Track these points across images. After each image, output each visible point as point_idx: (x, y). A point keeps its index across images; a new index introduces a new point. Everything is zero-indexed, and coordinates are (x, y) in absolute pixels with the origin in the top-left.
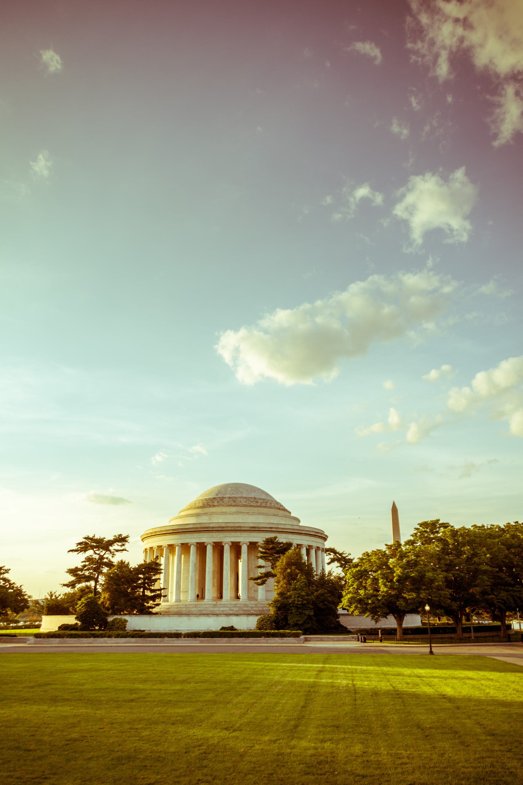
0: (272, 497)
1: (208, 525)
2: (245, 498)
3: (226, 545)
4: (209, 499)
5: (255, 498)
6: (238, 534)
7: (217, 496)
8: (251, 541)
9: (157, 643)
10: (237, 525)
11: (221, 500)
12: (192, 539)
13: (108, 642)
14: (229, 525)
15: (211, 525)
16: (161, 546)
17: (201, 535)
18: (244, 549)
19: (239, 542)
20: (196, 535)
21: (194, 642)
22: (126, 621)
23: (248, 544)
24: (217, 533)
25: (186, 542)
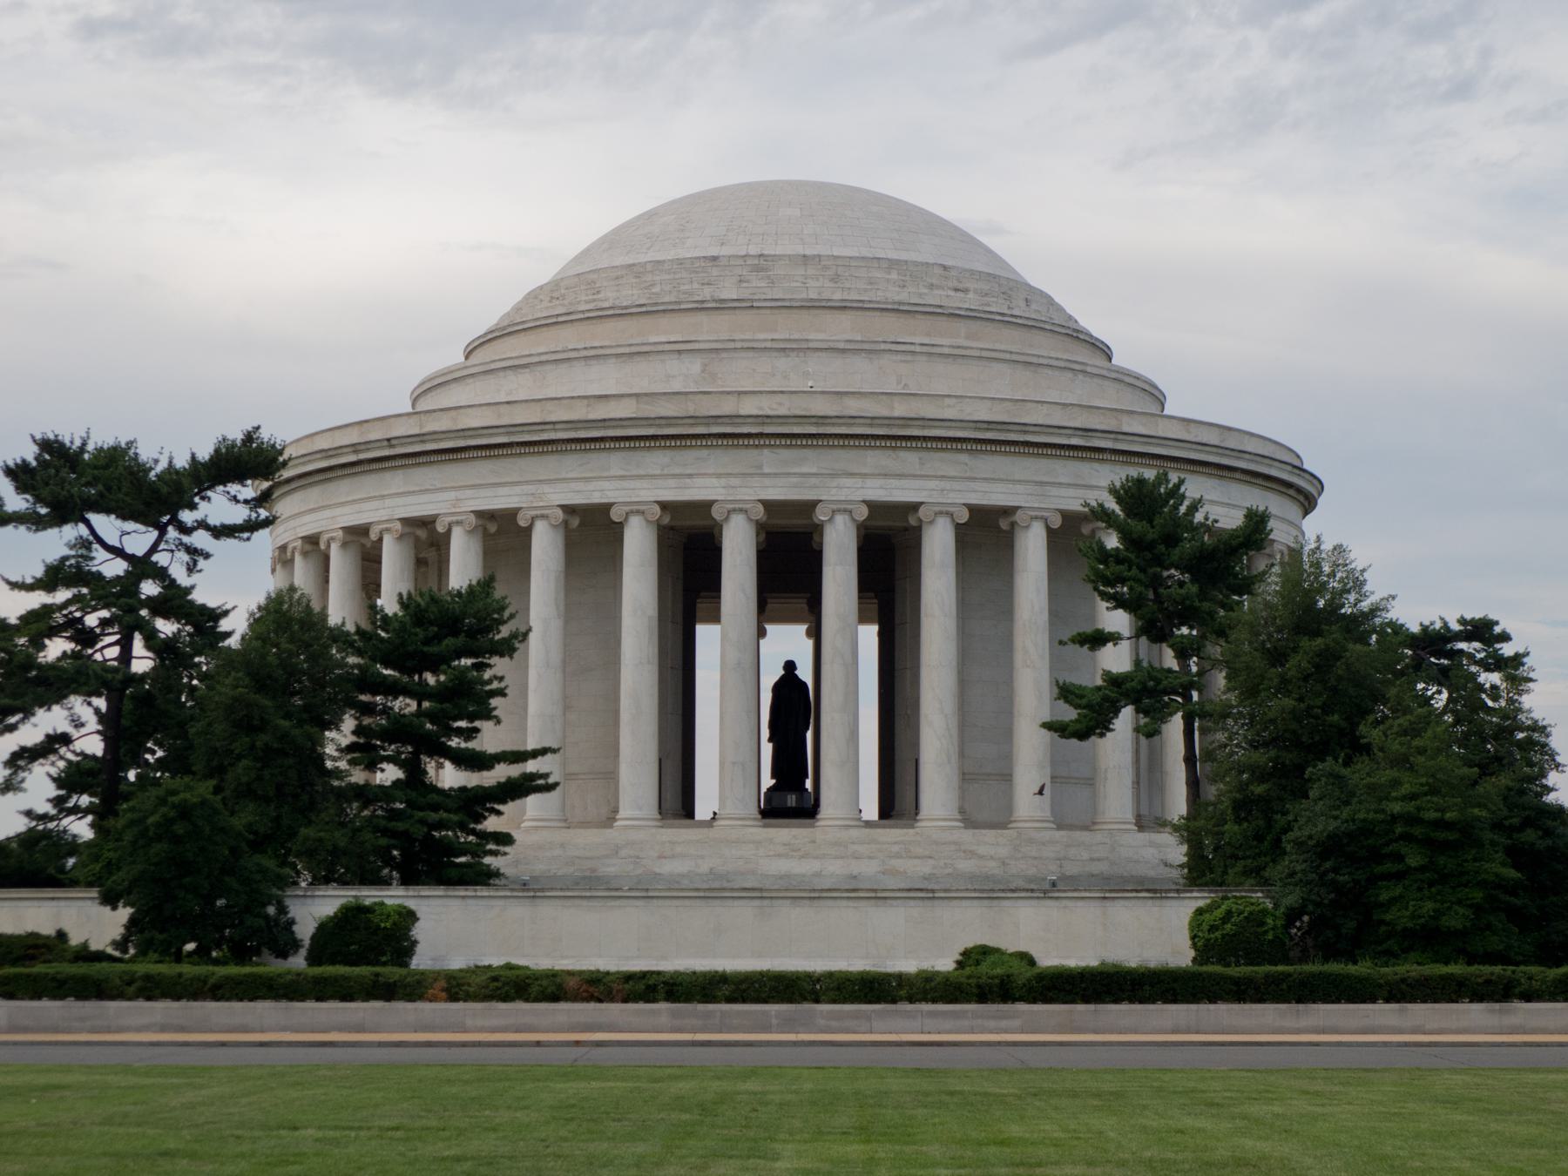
0: (1015, 272)
1: (727, 407)
2: (893, 264)
3: (840, 520)
4: (680, 262)
5: (945, 268)
6: (909, 459)
7: (725, 251)
8: (976, 499)
9: (767, 1029)
10: (900, 410)
11: (757, 269)
12: (637, 488)
13: (469, 1022)
14: (853, 407)
15: (749, 407)
16: (427, 523)
17: (690, 458)
18: (938, 548)
19: (914, 507)
20: (656, 460)
21: (992, 1024)
22: (410, 916)
23: (964, 517)
24: (785, 454)
25: (596, 498)
